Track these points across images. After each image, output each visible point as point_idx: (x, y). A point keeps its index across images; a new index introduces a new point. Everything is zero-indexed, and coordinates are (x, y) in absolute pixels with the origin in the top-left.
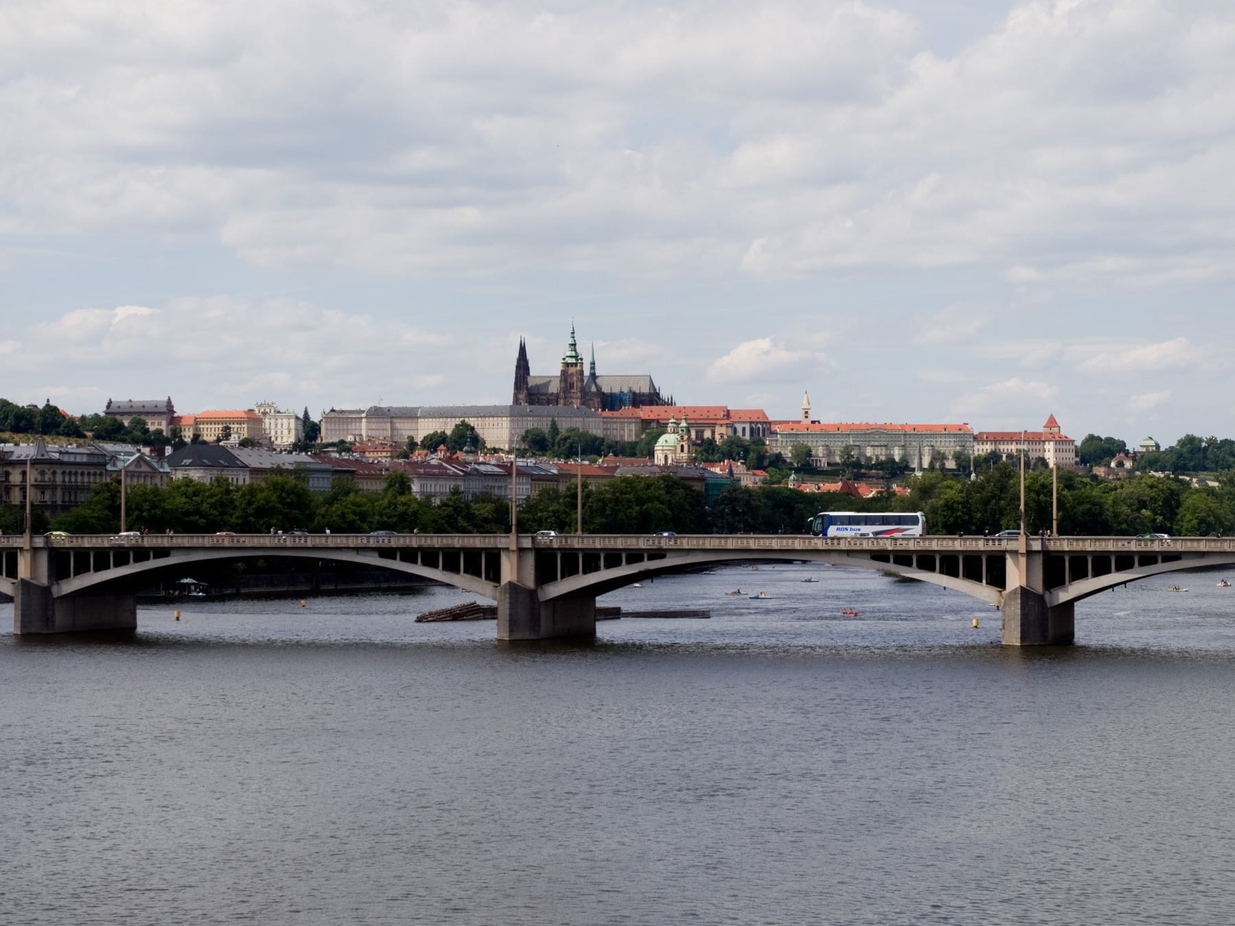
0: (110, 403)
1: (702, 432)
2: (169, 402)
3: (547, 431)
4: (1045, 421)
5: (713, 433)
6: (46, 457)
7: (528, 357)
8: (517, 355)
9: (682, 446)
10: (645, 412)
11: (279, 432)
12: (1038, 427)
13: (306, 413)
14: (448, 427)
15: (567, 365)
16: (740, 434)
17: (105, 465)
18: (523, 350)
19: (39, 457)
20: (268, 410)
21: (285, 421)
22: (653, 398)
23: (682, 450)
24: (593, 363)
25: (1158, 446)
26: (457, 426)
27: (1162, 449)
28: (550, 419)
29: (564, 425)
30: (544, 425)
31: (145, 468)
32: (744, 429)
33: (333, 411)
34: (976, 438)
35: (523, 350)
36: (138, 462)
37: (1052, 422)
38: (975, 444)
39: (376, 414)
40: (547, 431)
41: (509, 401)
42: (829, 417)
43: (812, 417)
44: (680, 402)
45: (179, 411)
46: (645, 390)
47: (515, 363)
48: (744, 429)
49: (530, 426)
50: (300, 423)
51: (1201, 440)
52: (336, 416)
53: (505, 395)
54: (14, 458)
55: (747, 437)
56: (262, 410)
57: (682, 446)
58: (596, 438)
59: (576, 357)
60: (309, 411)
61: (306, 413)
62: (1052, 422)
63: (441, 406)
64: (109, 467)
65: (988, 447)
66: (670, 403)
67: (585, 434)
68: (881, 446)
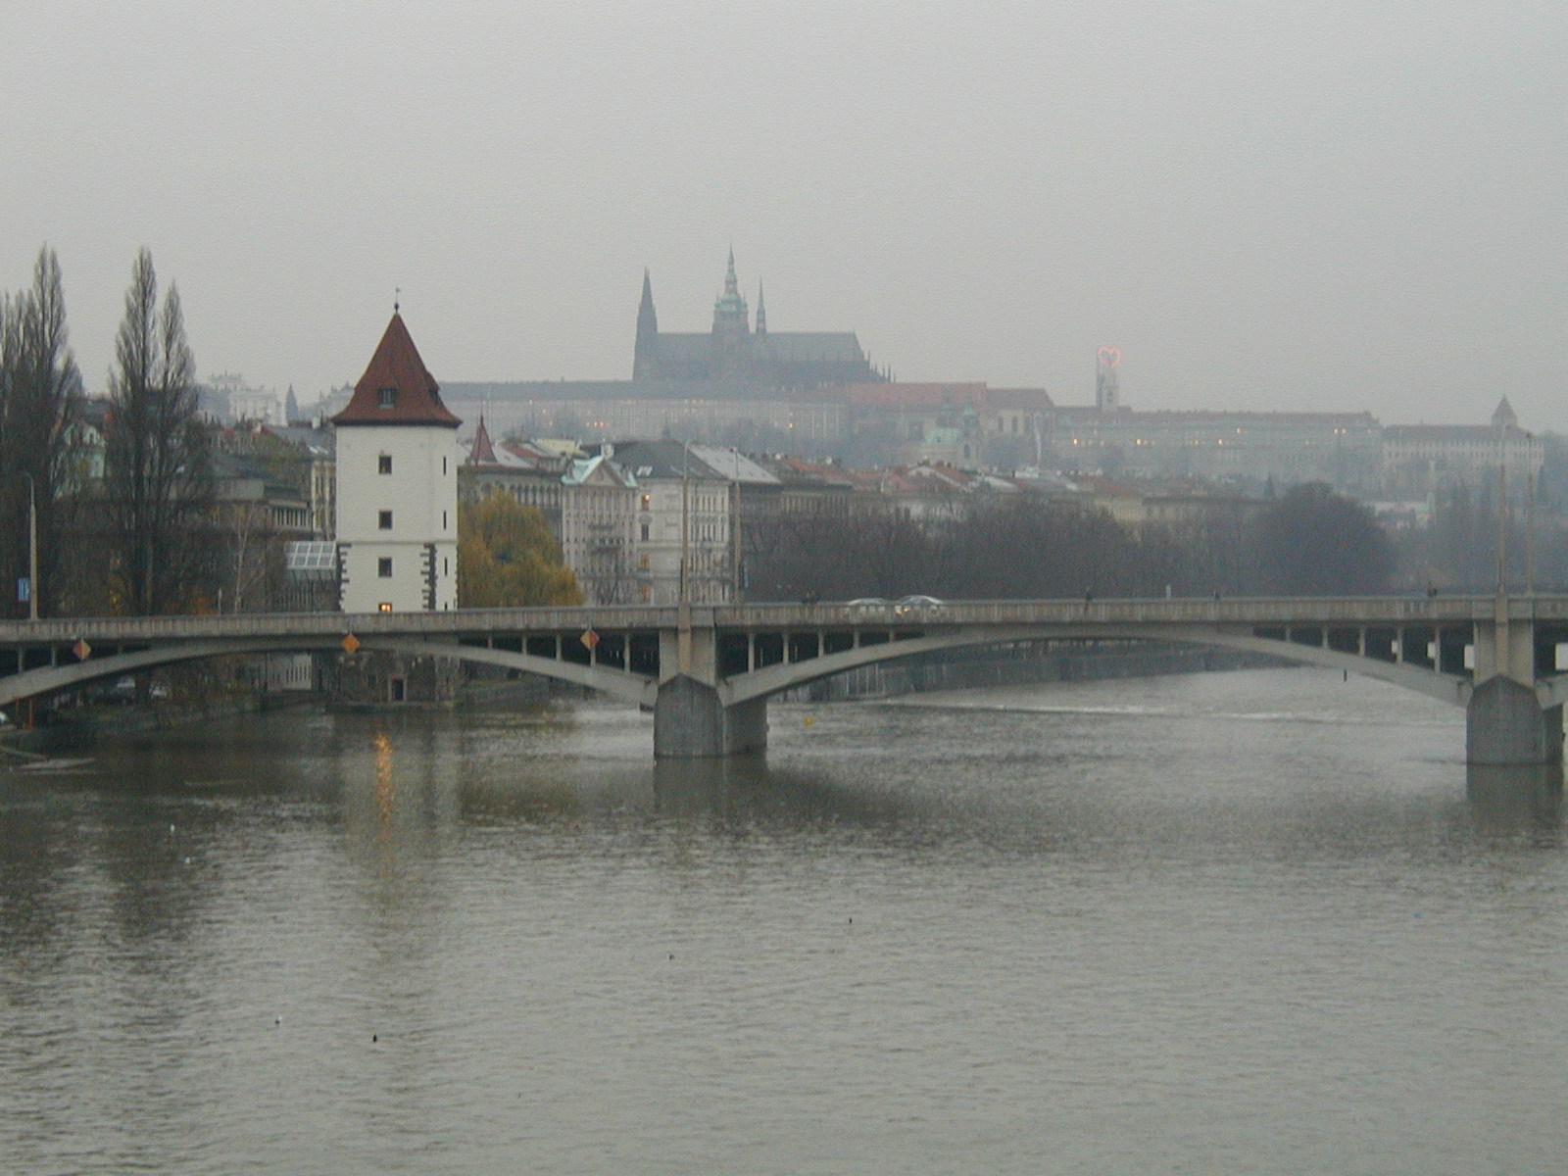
8: (639, 299)
12: (1484, 417)
16: (1008, 427)
17: (560, 475)
24: (761, 312)
31: (608, 482)
37: (1504, 410)
41: (627, 375)
48: (1015, 421)
57: (967, 447)
60: (295, 390)
62: (1504, 410)
63: (509, 380)
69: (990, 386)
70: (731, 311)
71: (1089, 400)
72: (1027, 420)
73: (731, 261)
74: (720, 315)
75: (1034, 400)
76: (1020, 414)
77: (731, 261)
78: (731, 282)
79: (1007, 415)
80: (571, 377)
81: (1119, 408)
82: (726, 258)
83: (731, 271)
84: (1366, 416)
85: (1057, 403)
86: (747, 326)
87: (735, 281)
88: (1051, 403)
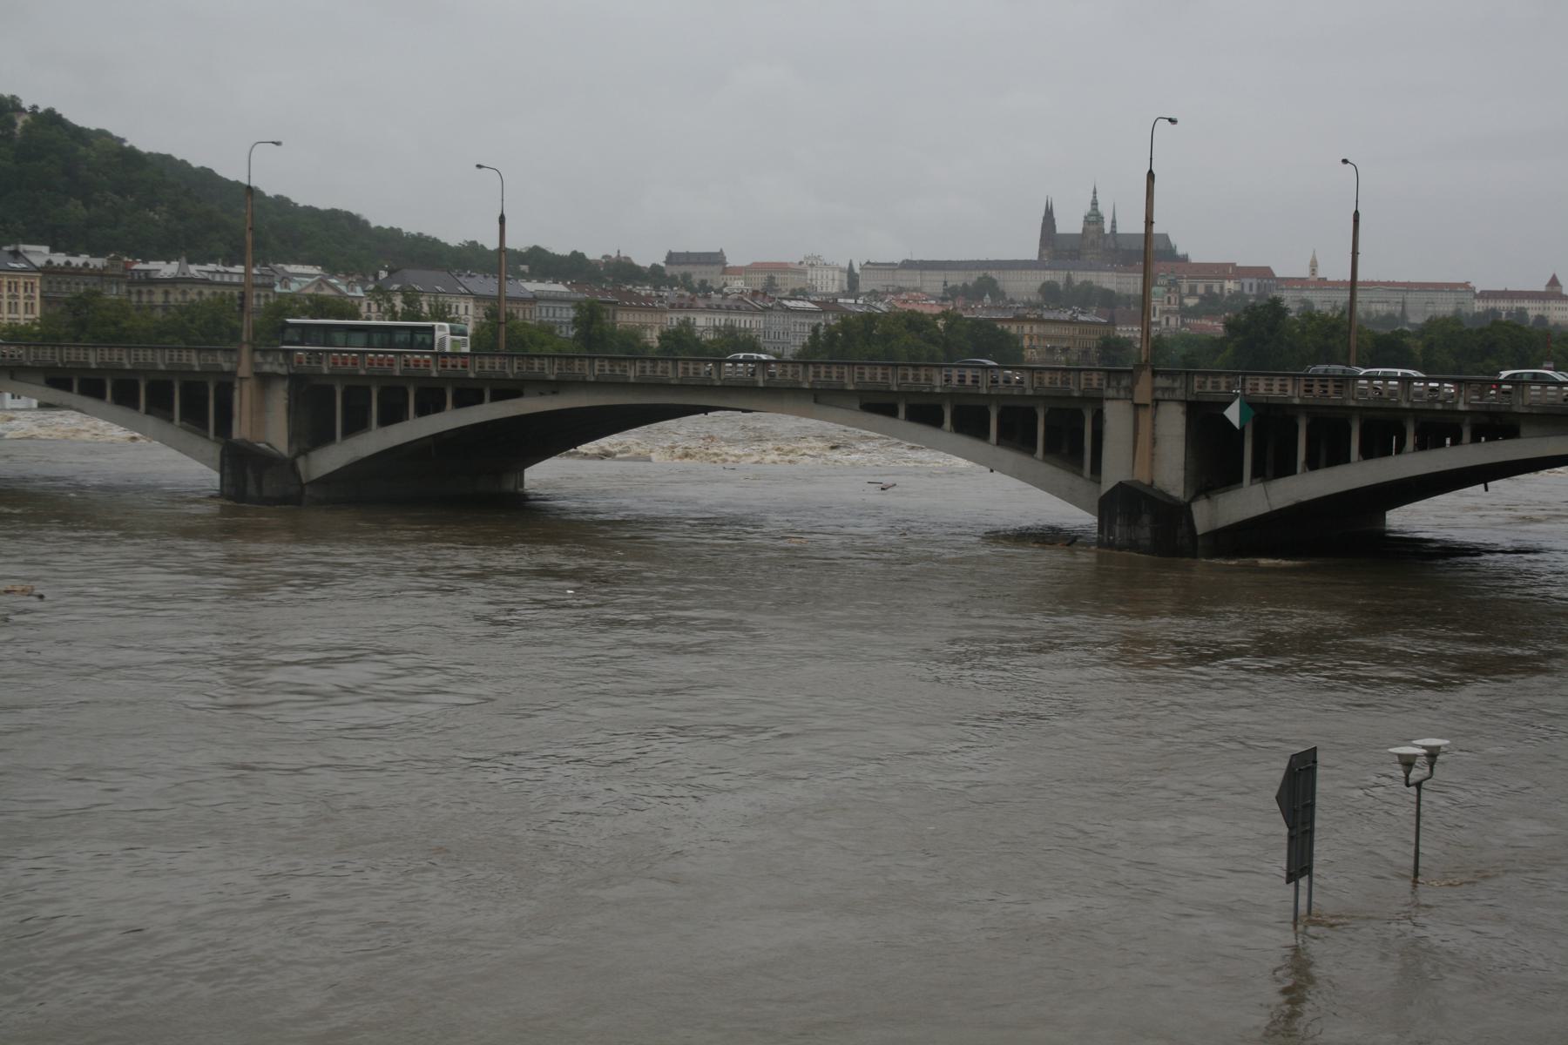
1: (1196, 287)
2: (721, 250)
3: (1061, 284)
4: (1549, 278)
5: (1222, 288)
6: (188, 276)
7: (1055, 215)
9: (1169, 298)
11: (825, 283)
12: (1541, 286)
13: (851, 265)
14: (972, 277)
16: (1246, 290)
19: (180, 275)
20: (815, 263)
21: (830, 273)
24: (1114, 222)
26: (979, 279)
28: (1066, 273)
29: (1079, 277)
30: (1059, 277)
32: (1251, 285)
33: (868, 263)
36: (320, 285)
37: (1554, 281)
38: (1476, 301)
39: (908, 265)
40: (1061, 284)
43: (1320, 274)
44: (1195, 258)
45: (732, 261)
47: (1041, 221)
48: (1251, 285)
49: (1048, 278)
50: (846, 275)
52: (871, 266)
53: (1028, 247)
54: (158, 276)
55: (1254, 291)
56: (810, 262)
57: (1169, 298)
58: (1107, 290)
61: (851, 265)
62: (1554, 281)
64: (278, 289)
65: (1491, 304)
66: (1185, 259)
67: (1101, 288)
68: (1382, 302)
69: (1238, 265)
70: (1094, 218)
71: (1303, 272)
72: (1259, 286)
73: (1095, 193)
74: (1087, 221)
75: (1265, 273)
76: (1255, 282)
77: (1095, 193)
78: (1095, 203)
79: (1247, 282)
80: (992, 258)
81: (1319, 279)
82: (1092, 189)
83: (1095, 197)
84: (1466, 285)
85: (1278, 275)
86: (1104, 230)
87: (1097, 204)
88: (1273, 275)
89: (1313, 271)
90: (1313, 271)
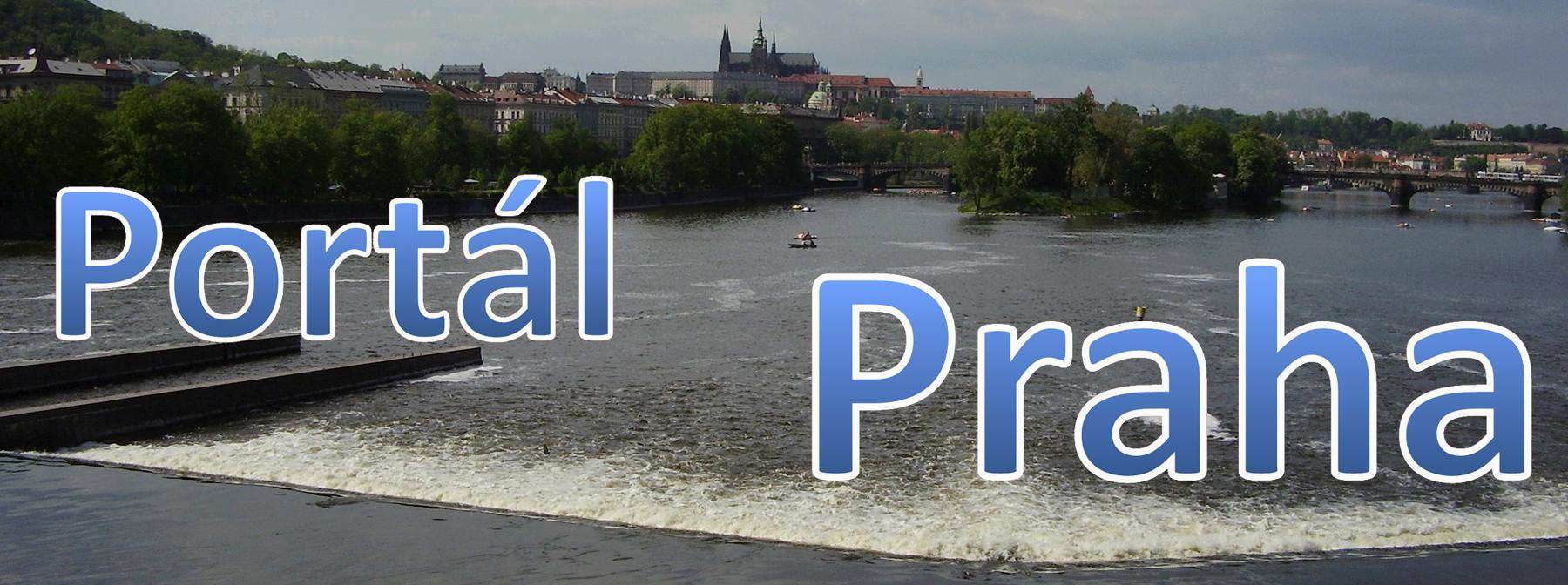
0: (442, 66)
9: (828, 101)
10: (807, 79)
15: (756, 44)
18: (726, 35)
22: (812, 68)
23: (828, 104)
24: (774, 44)
25: (1158, 111)
27: (1161, 113)
33: (593, 74)
34: (1037, 102)
35: (726, 35)
42: (934, 83)
46: (809, 63)
51: (1186, 108)
57: (828, 101)
59: (762, 40)
60: (580, 75)
66: (825, 73)
70: (759, 46)
89: (920, 82)
90: (920, 82)
